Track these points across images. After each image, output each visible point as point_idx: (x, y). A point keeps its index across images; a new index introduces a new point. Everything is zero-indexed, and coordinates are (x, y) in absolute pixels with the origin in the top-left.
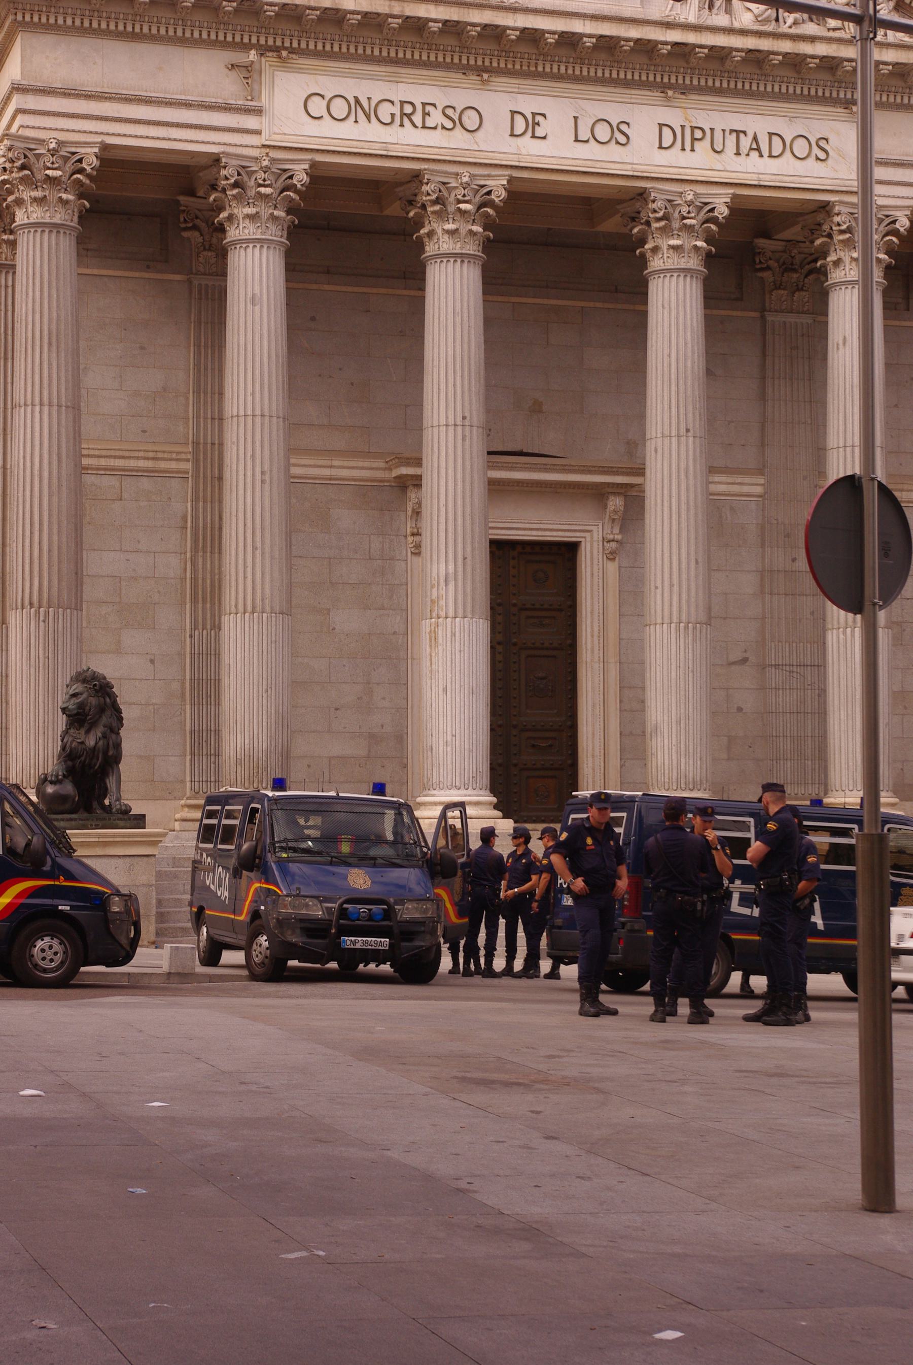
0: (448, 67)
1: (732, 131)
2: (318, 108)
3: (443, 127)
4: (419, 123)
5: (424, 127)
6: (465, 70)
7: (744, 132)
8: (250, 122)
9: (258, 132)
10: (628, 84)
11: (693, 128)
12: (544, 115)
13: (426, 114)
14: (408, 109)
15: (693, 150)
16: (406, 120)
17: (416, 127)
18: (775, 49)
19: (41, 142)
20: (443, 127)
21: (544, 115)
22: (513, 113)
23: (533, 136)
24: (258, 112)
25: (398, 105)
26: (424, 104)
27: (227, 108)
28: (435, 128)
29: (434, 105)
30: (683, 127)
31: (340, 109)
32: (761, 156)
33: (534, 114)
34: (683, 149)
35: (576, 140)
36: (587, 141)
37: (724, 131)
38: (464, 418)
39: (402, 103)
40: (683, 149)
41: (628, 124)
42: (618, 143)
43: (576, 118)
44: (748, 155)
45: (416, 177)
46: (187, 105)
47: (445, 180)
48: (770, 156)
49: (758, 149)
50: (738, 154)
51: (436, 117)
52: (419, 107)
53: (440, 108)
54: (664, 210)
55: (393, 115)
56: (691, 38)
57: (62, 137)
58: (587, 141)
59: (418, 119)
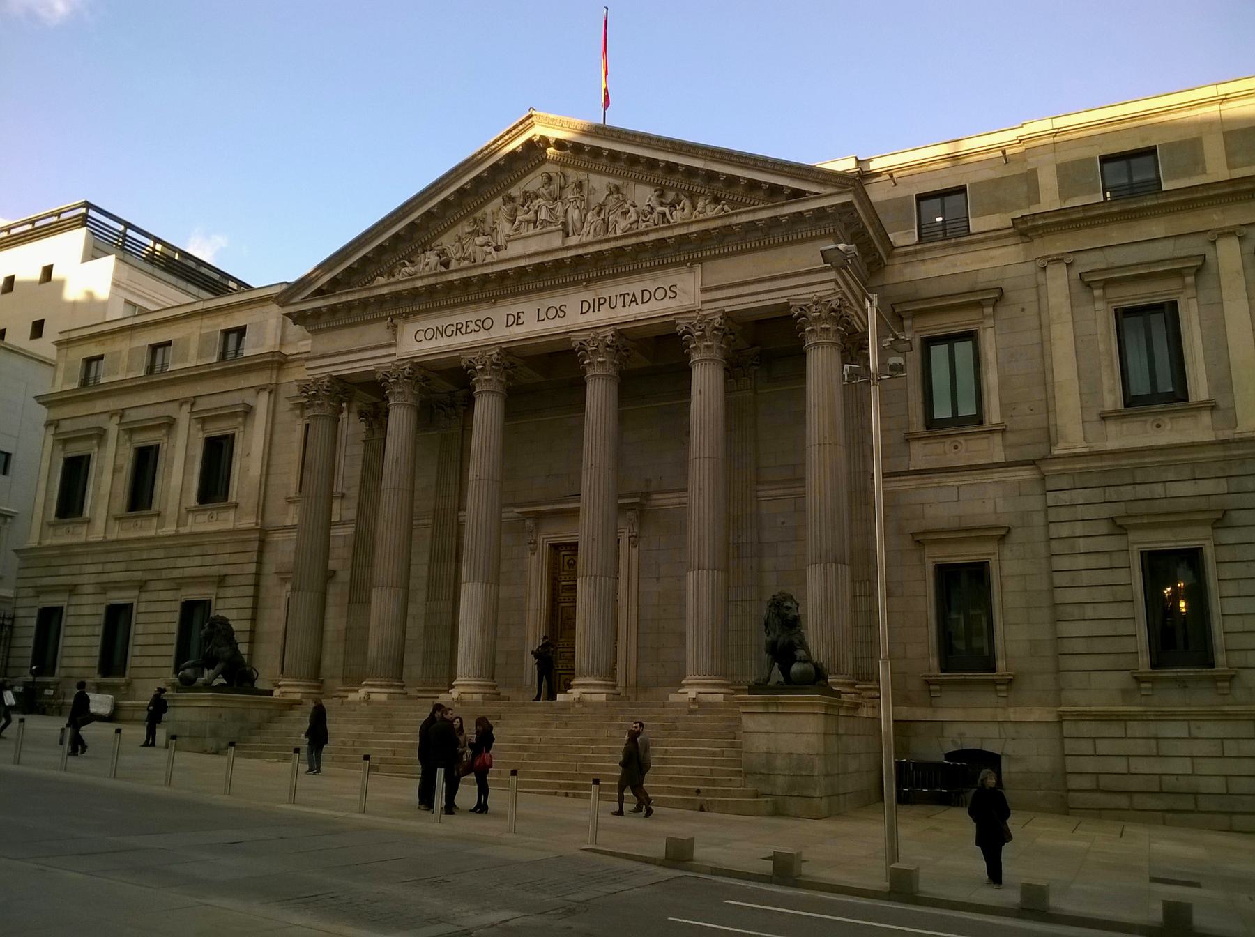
0: (479, 301)
1: (621, 295)
2: (421, 336)
3: (475, 331)
4: (464, 332)
5: (466, 333)
6: (487, 300)
7: (628, 294)
8: (392, 351)
9: (395, 354)
10: (567, 285)
11: (599, 299)
12: (523, 312)
13: (467, 326)
14: (459, 326)
15: (599, 310)
16: (458, 331)
17: (462, 334)
18: (626, 244)
19: (309, 380)
20: (475, 331)
21: (523, 312)
22: (508, 315)
23: (517, 324)
24: (394, 345)
25: (455, 325)
26: (467, 322)
27: (382, 347)
28: (471, 332)
29: (471, 321)
30: (594, 300)
31: (429, 335)
32: (637, 304)
33: (518, 313)
34: (594, 311)
35: (538, 321)
36: (544, 320)
37: (616, 296)
38: (477, 476)
39: (457, 324)
40: (594, 311)
41: (565, 306)
42: (559, 317)
43: (539, 310)
44: (630, 305)
45: (459, 358)
46: (366, 349)
47: (473, 357)
48: (643, 303)
49: (636, 301)
50: (624, 306)
51: (472, 327)
52: (465, 324)
53: (474, 322)
54: (579, 346)
55: (453, 331)
56: (580, 251)
57: (317, 377)
58: (544, 320)
59: (463, 330)
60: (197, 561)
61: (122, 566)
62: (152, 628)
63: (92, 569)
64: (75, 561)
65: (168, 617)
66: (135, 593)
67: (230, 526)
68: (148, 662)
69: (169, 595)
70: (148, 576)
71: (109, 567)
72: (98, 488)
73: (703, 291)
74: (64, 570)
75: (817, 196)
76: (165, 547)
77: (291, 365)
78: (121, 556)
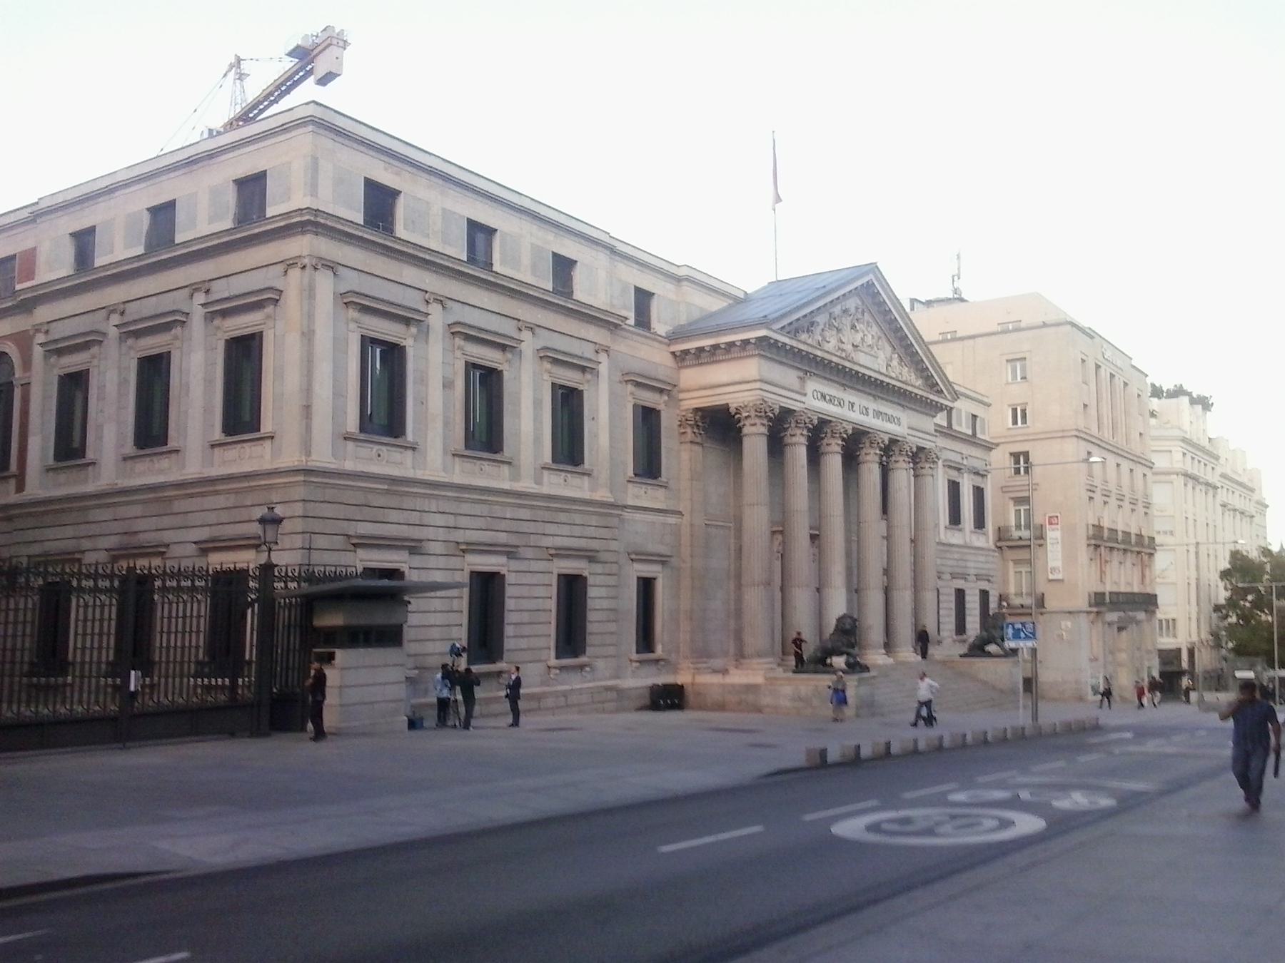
60: (565, 530)
61: (480, 523)
62: (526, 604)
63: (440, 520)
64: (409, 503)
65: (541, 592)
66: (502, 560)
67: (586, 495)
68: (523, 643)
69: (541, 566)
70: (513, 540)
71: (463, 522)
72: (422, 402)
73: (909, 428)
74: (394, 516)
75: (946, 398)
76: (532, 507)
77: (624, 333)
78: (477, 509)
